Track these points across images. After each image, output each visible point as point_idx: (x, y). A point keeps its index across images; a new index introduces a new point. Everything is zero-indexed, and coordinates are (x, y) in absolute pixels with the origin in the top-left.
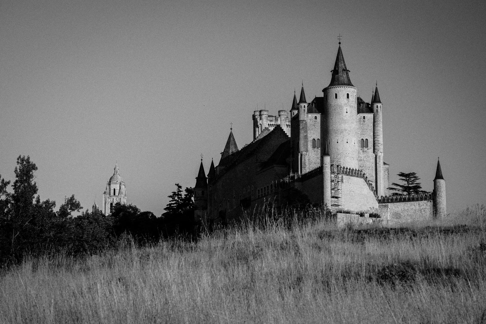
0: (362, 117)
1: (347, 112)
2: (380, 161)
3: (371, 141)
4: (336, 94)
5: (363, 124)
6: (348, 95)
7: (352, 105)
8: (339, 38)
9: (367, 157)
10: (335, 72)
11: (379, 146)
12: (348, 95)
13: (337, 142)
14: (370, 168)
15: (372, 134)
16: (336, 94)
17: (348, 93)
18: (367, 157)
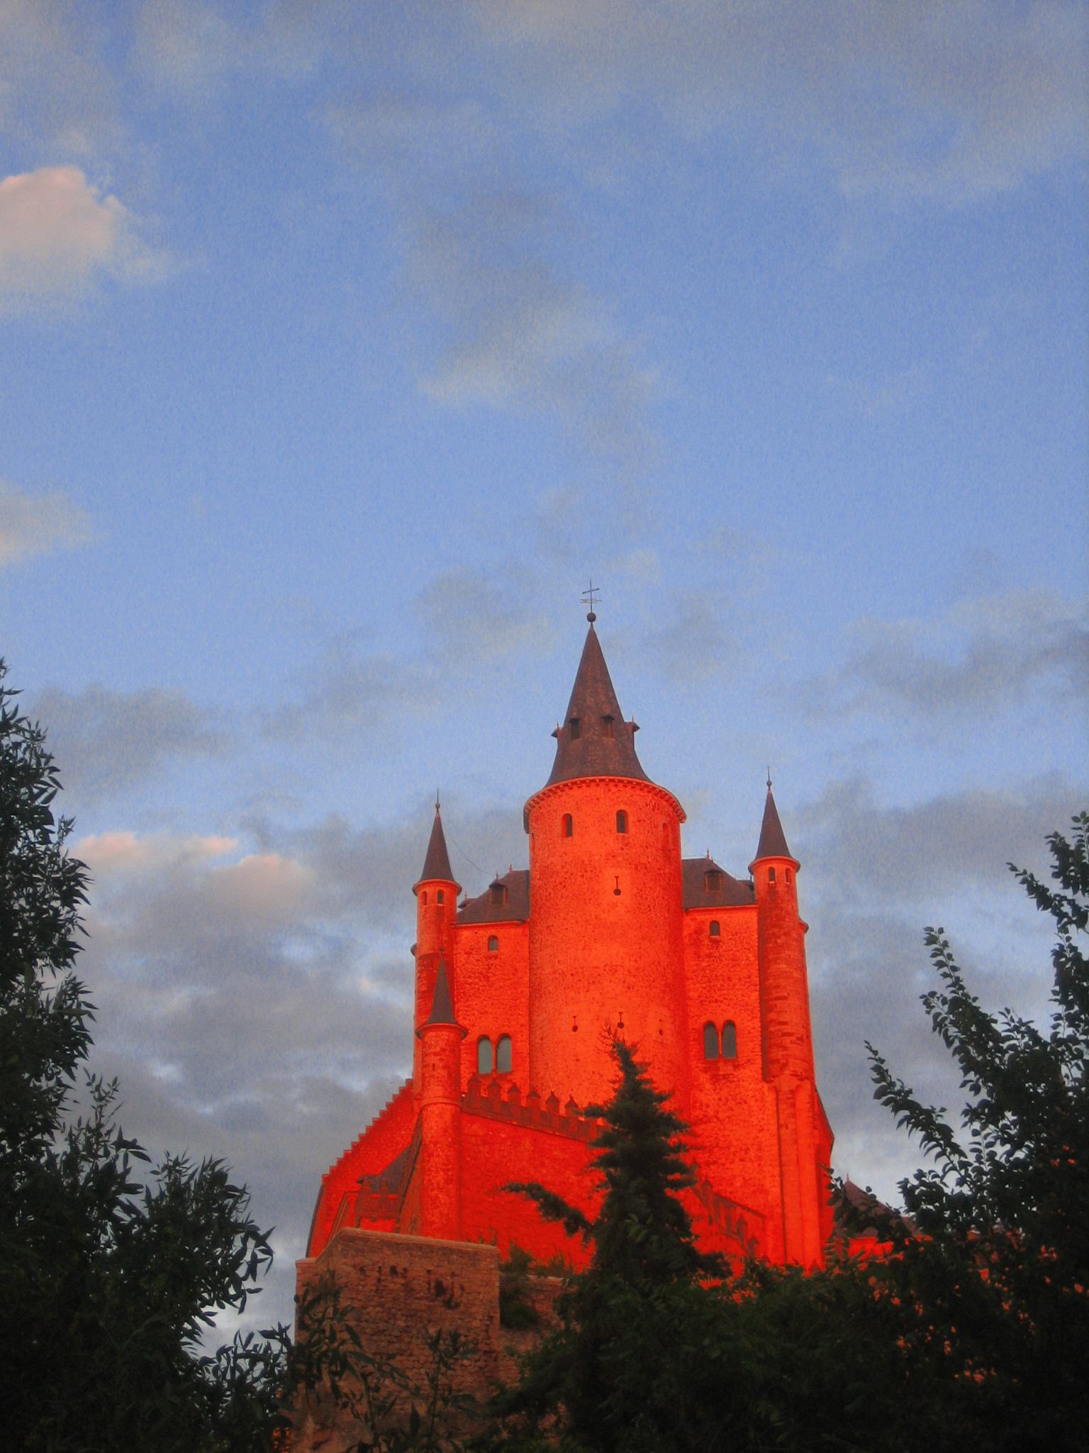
0: (707, 927)
1: (617, 892)
2: (794, 1116)
3: (749, 1024)
4: (568, 819)
5: (709, 956)
6: (622, 816)
7: (644, 860)
8: (587, 596)
9: (731, 1103)
10: (572, 731)
11: (785, 1048)
12: (622, 816)
13: (575, 1029)
14: (752, 1154)
15: (755, 996)
16: (568, 819)
17: (623, 807)
18: (731, 1103)
